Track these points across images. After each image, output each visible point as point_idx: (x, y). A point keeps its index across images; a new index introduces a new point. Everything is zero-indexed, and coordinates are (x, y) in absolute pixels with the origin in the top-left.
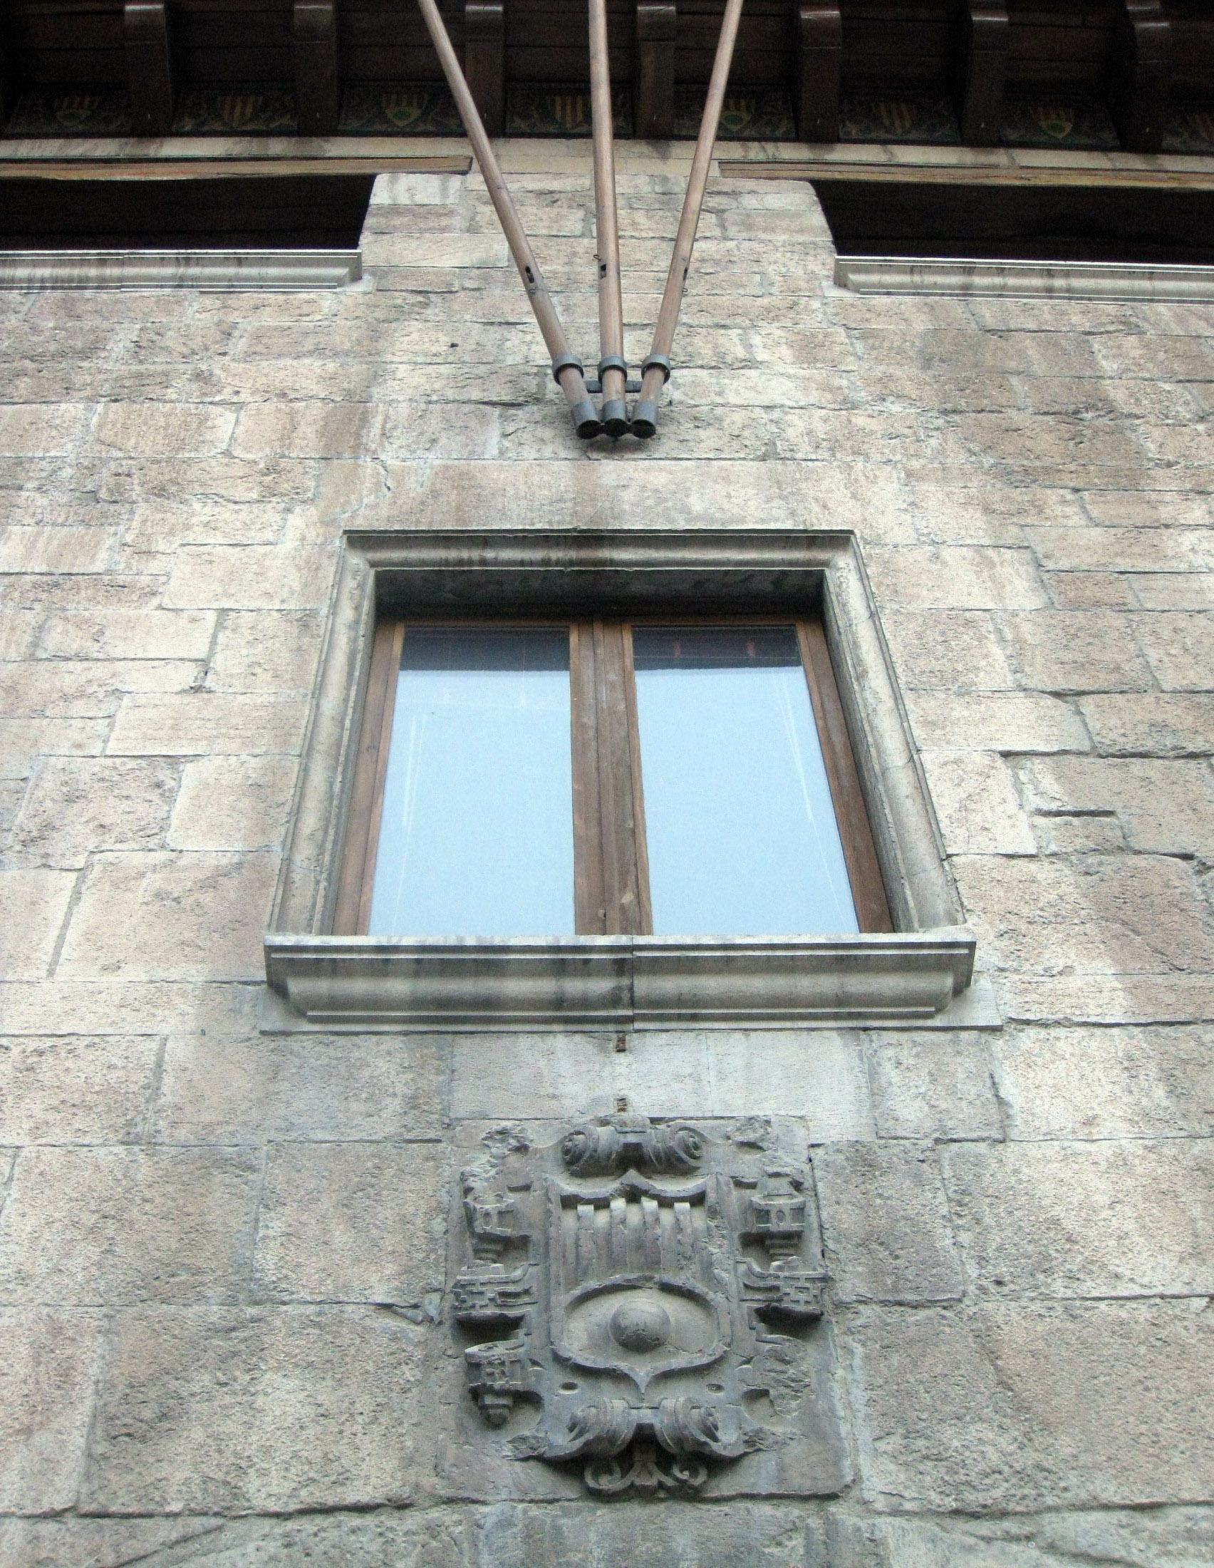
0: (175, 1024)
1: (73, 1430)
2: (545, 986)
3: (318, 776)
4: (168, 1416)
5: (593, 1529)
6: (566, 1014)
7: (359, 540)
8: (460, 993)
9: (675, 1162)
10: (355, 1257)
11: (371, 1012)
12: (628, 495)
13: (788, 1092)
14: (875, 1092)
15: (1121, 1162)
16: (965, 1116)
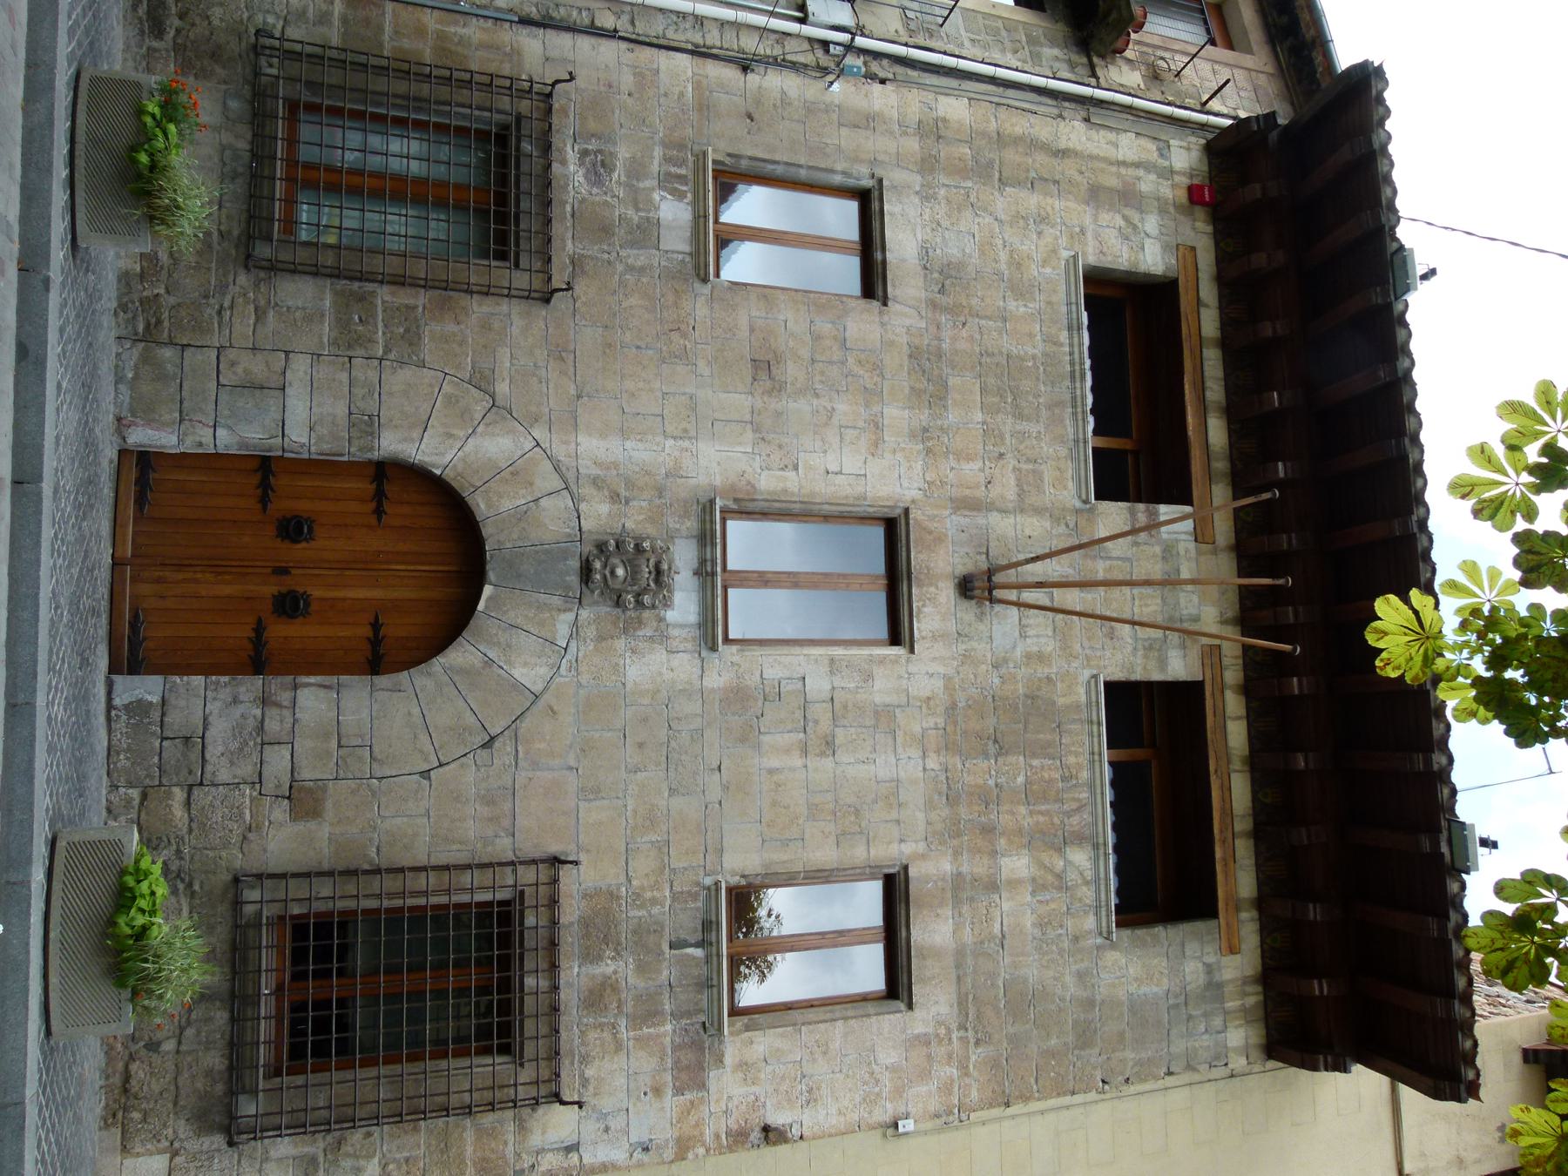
0: (702, 480)
1: (596, 471)
2: (709, 556)
3: (798, 506)
4: (599, 488)
5: (575, 564)
6: (702, 562)
7: (907, 511)
8: (708, 539)
9: (657, 581)
10: (634, 521)
11: (703, 522)
12: (932, 589)
13: (683, 606)
14: (682, 626)
15: (660, 674)
16: (674, 644)
